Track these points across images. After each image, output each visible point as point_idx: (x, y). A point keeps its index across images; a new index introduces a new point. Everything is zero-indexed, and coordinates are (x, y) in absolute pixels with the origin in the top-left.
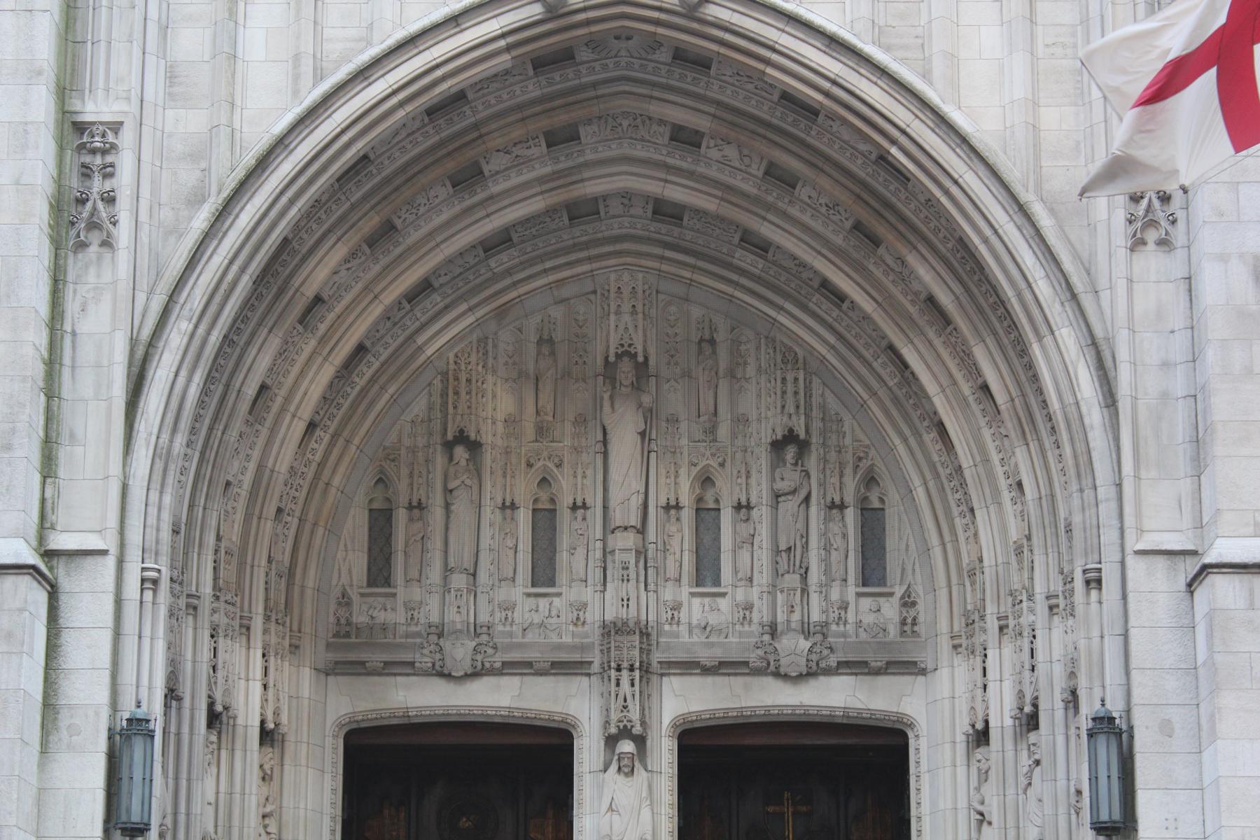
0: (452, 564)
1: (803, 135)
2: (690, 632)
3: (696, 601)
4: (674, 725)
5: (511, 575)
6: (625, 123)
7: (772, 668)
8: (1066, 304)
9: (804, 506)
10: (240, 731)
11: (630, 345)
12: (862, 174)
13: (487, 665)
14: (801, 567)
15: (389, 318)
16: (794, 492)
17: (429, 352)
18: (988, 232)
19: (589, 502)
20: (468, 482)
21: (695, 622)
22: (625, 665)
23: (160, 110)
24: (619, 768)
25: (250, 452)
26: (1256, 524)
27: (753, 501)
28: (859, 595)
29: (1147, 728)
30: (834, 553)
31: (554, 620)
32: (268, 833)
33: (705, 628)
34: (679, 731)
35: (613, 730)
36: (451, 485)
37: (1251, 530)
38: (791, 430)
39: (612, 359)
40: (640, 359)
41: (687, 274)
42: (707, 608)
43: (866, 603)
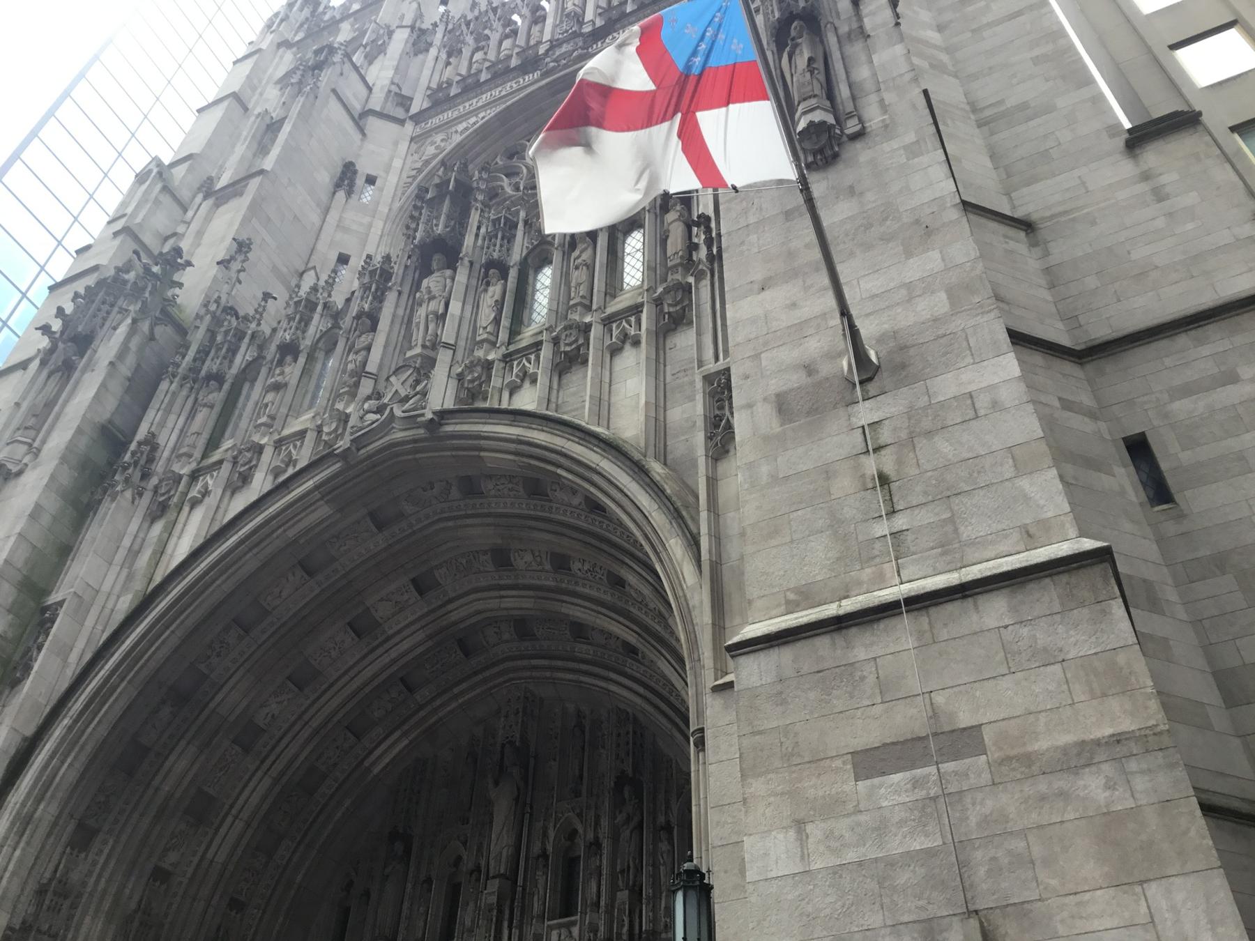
1: (548, 515)
6: (464, 561)
8: (673, 521)
11: (512, 737)
12: (584, 525)
14: (635, 882)
15: (337, 748)
16: (629, 819)
17: (376, 771)
18: (618, 496)
23: (113, 598)
26: (788, 602)
29: (726, 872)
30: (662, 868)
37: (783, 607)
38: (623, 772)
41: (548, 674)
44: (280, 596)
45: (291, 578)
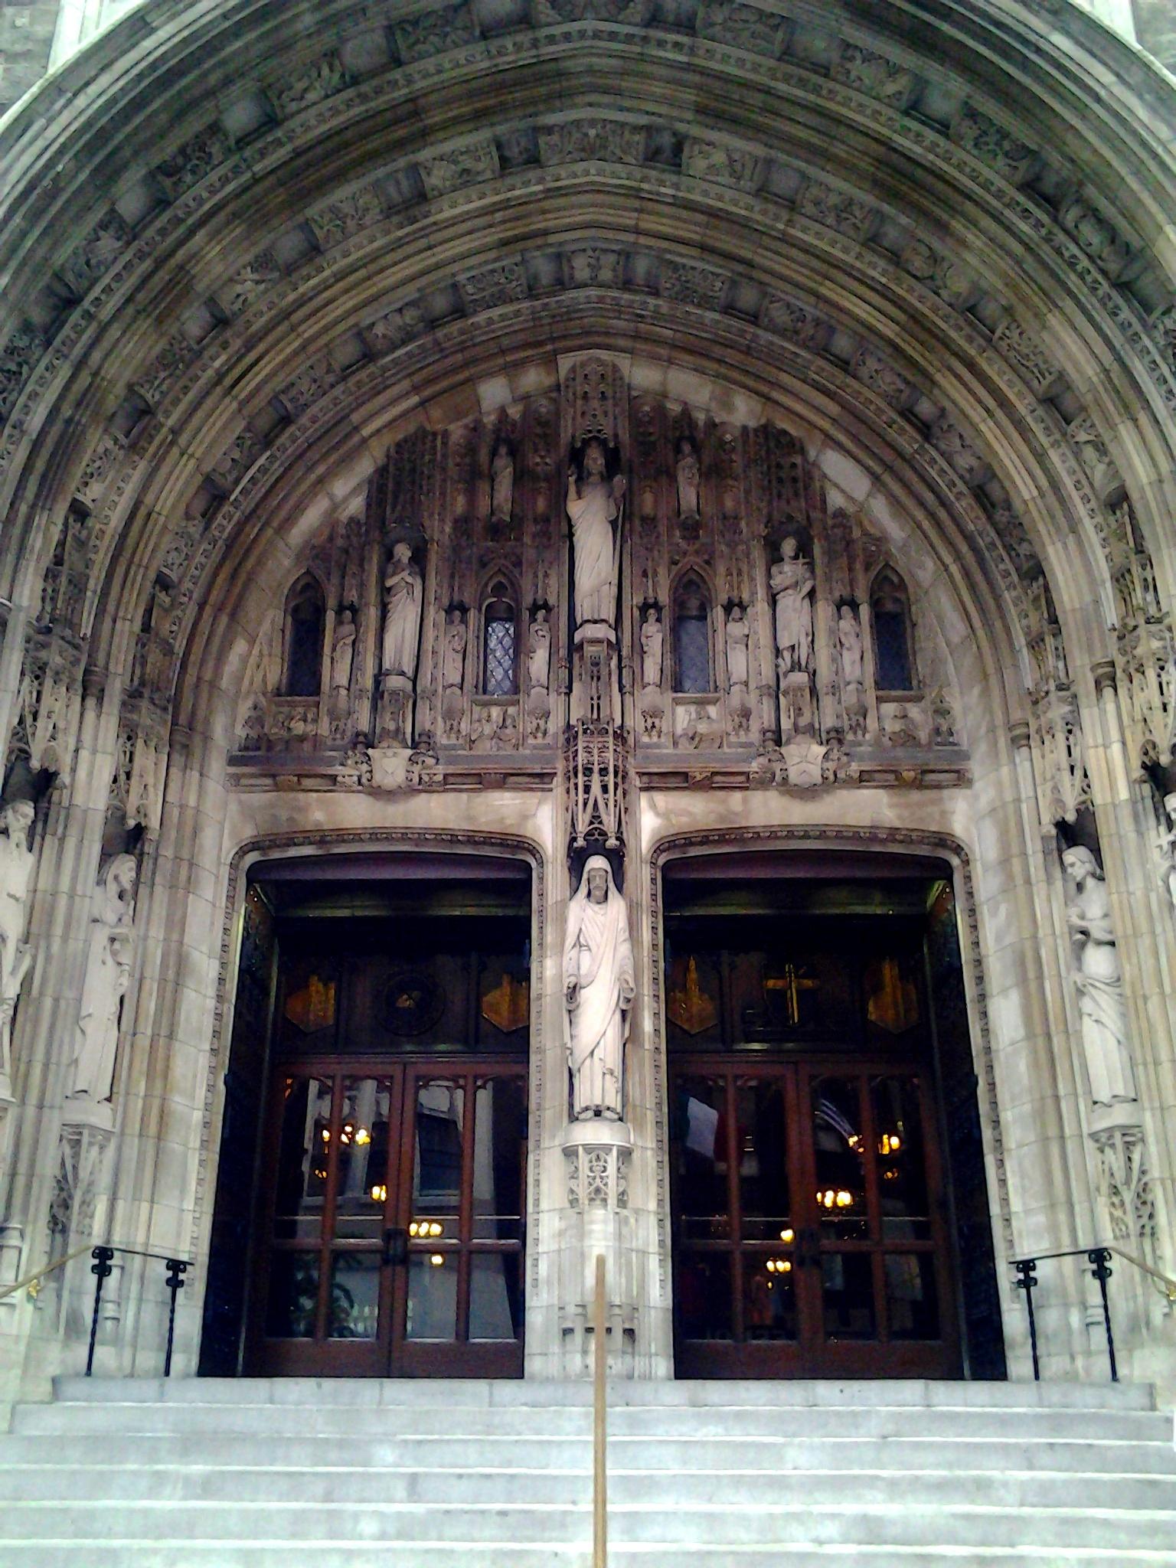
0: (387, 665)
2: (675, 744)
3: (680, 710)
4: (659, 849)
5: (458, 680)
6: (592, 132)
7: (778, 778)
9: (807, 601)
10: (77, 813)
11: (599, 431)
13: (426, 778)
15: (315, 381)
19: (552, 601)
20: (409, 580)
21: (679, 731)
22: (596, 768)
24: (589, 894)
25: (122, 484)
27: (746, 596)
28: (880, 700)
31: (509, 731)
32: (120, 964)
33: (693, 738)
34: (662, 860)
35: (580, 842)
36: (389, 583)
39: (579, 445)
40: (611, 445)
42: (694, 716)
43: (890, 708)
44: (302, 98)
45: (325, 71)
